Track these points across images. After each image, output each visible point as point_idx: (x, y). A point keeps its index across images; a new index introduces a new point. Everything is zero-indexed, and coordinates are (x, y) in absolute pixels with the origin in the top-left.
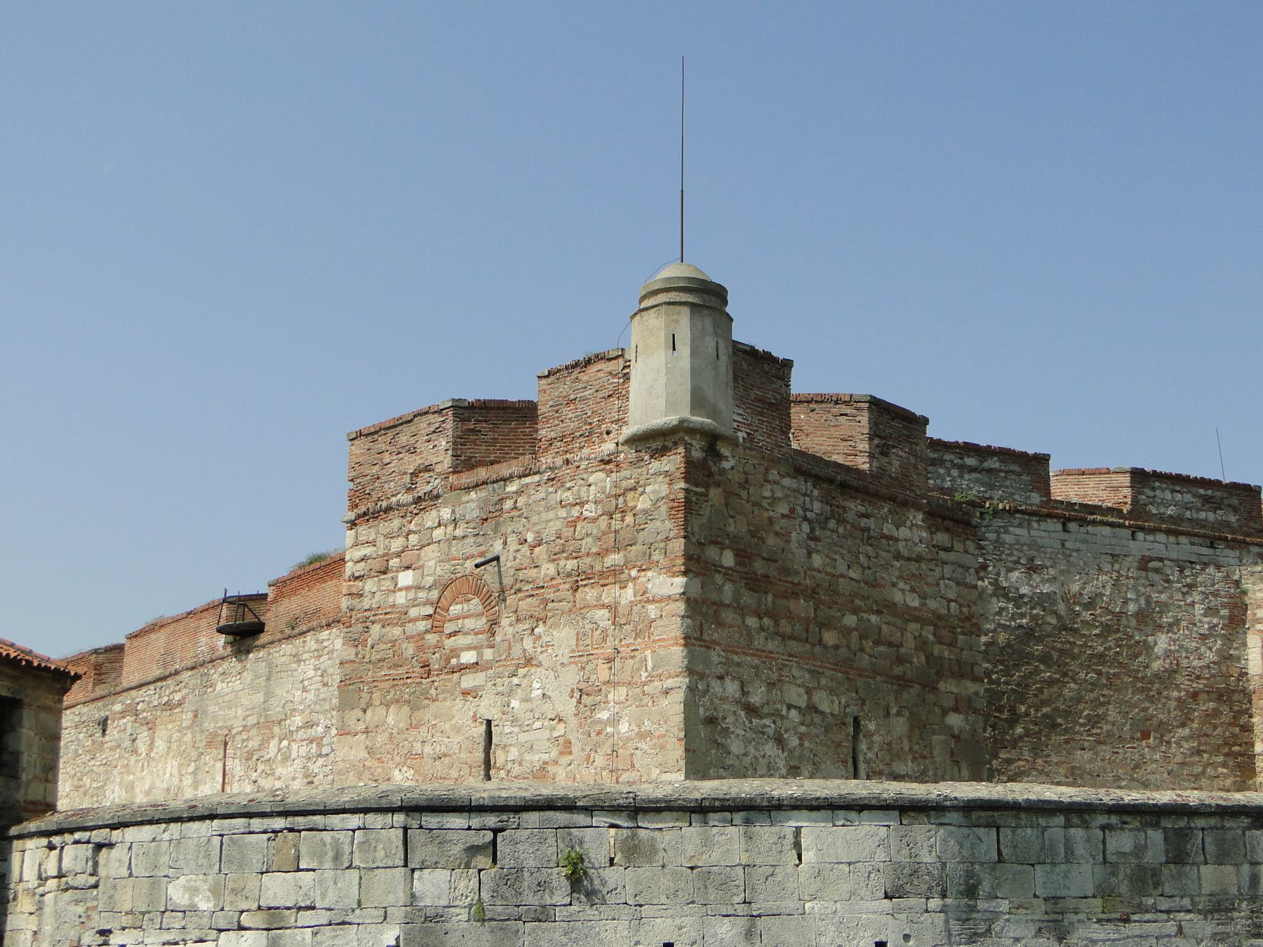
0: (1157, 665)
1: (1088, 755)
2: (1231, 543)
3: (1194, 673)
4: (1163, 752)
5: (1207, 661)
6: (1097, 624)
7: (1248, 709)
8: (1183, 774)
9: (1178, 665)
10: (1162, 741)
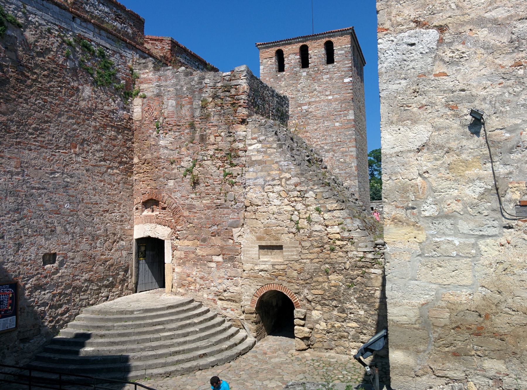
0: (83, 104)
1: (33, 154)
2: (128, 45)
3: (105, 114)
4: (84, 158)
5: (112, 108)
6: (46, 68)
7: (131, 139)
8: (95, 172)
9: (96, 107)
10: (83, 150)
